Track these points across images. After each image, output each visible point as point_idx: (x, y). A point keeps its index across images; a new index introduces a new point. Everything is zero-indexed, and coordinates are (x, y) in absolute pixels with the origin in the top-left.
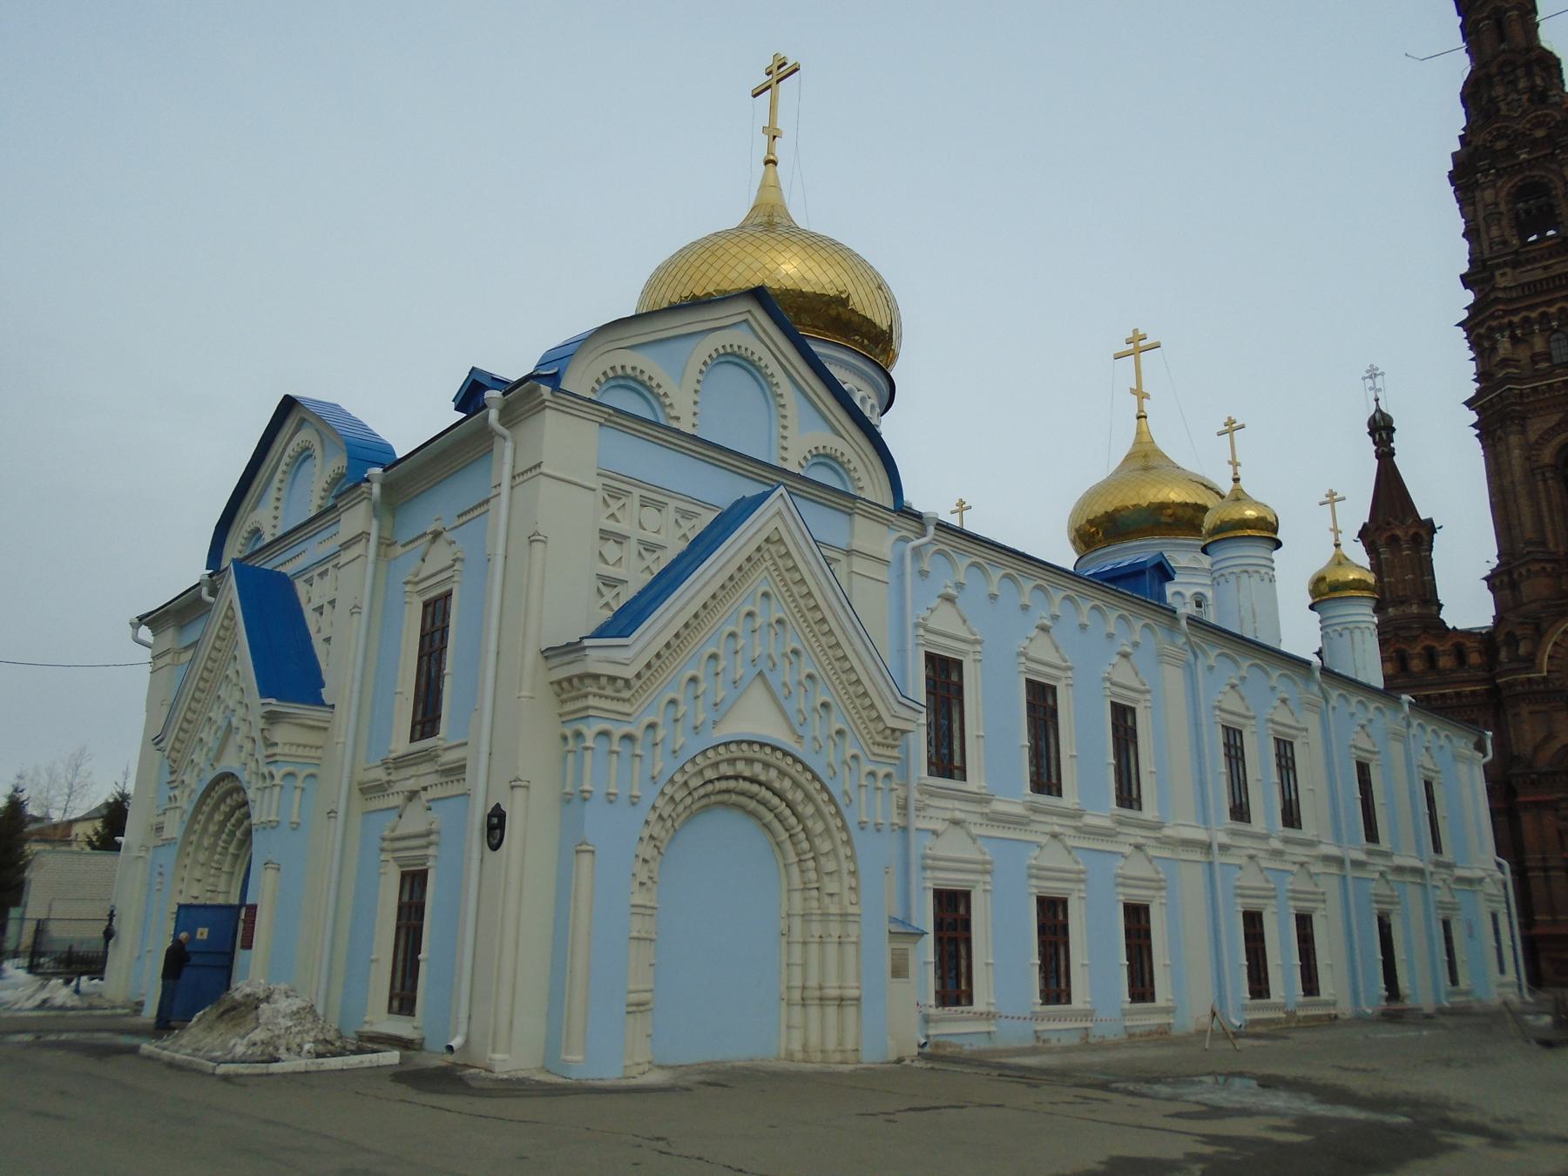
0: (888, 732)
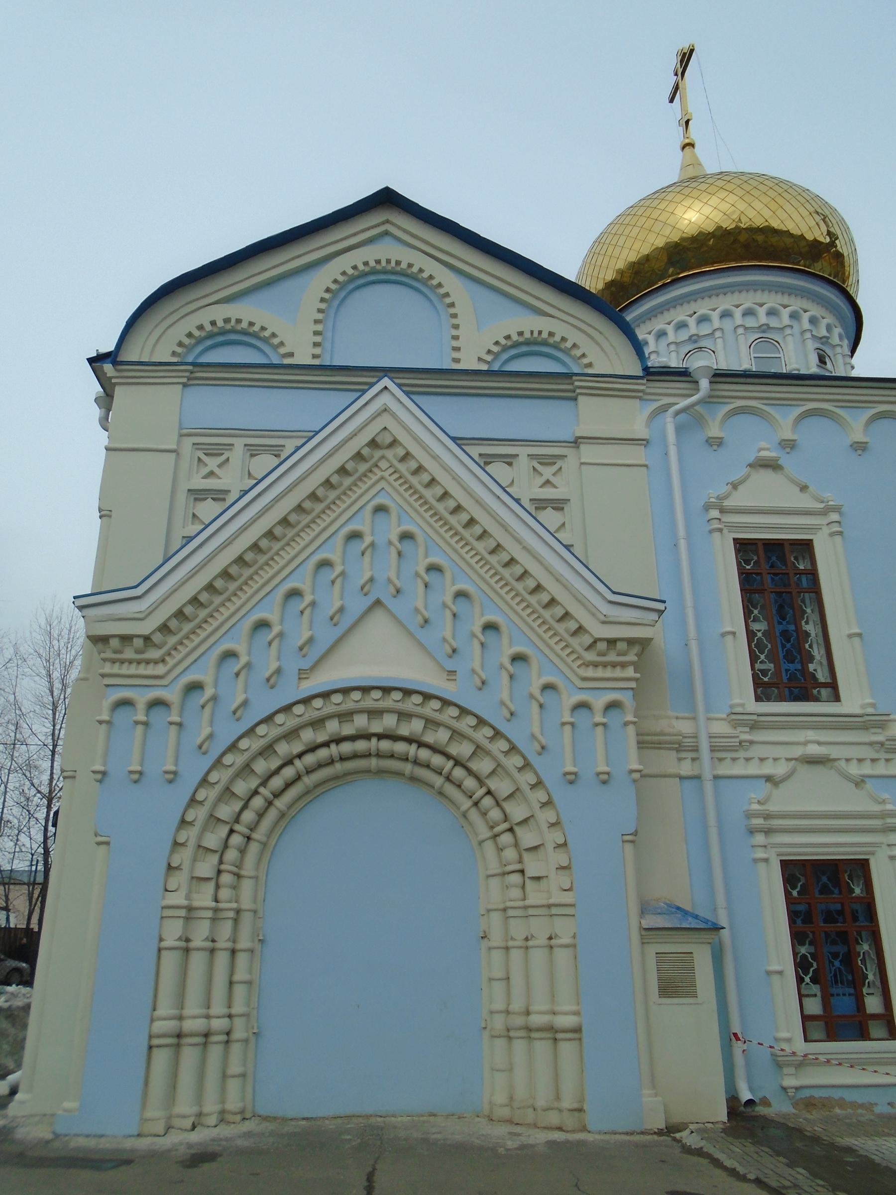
0: (602, 646)
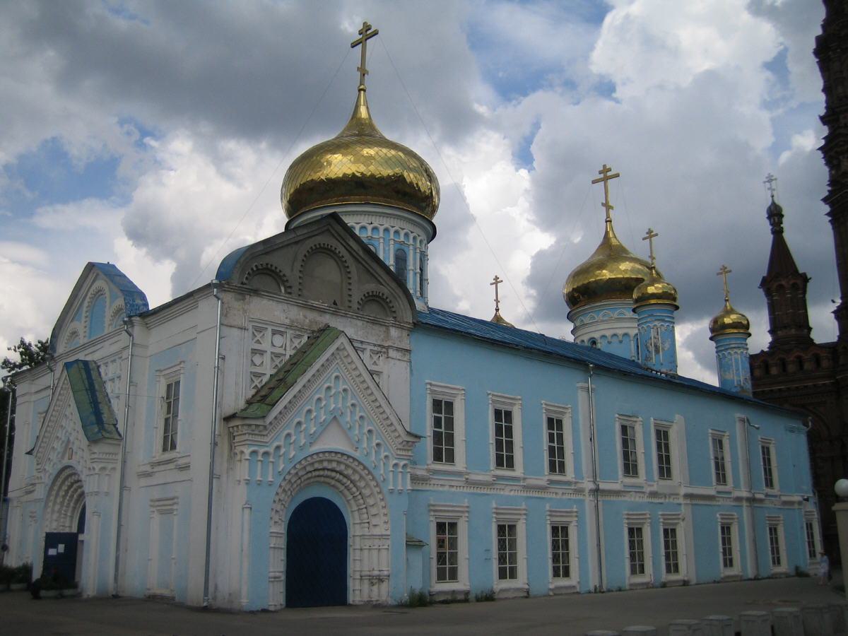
0: (404, 443)
